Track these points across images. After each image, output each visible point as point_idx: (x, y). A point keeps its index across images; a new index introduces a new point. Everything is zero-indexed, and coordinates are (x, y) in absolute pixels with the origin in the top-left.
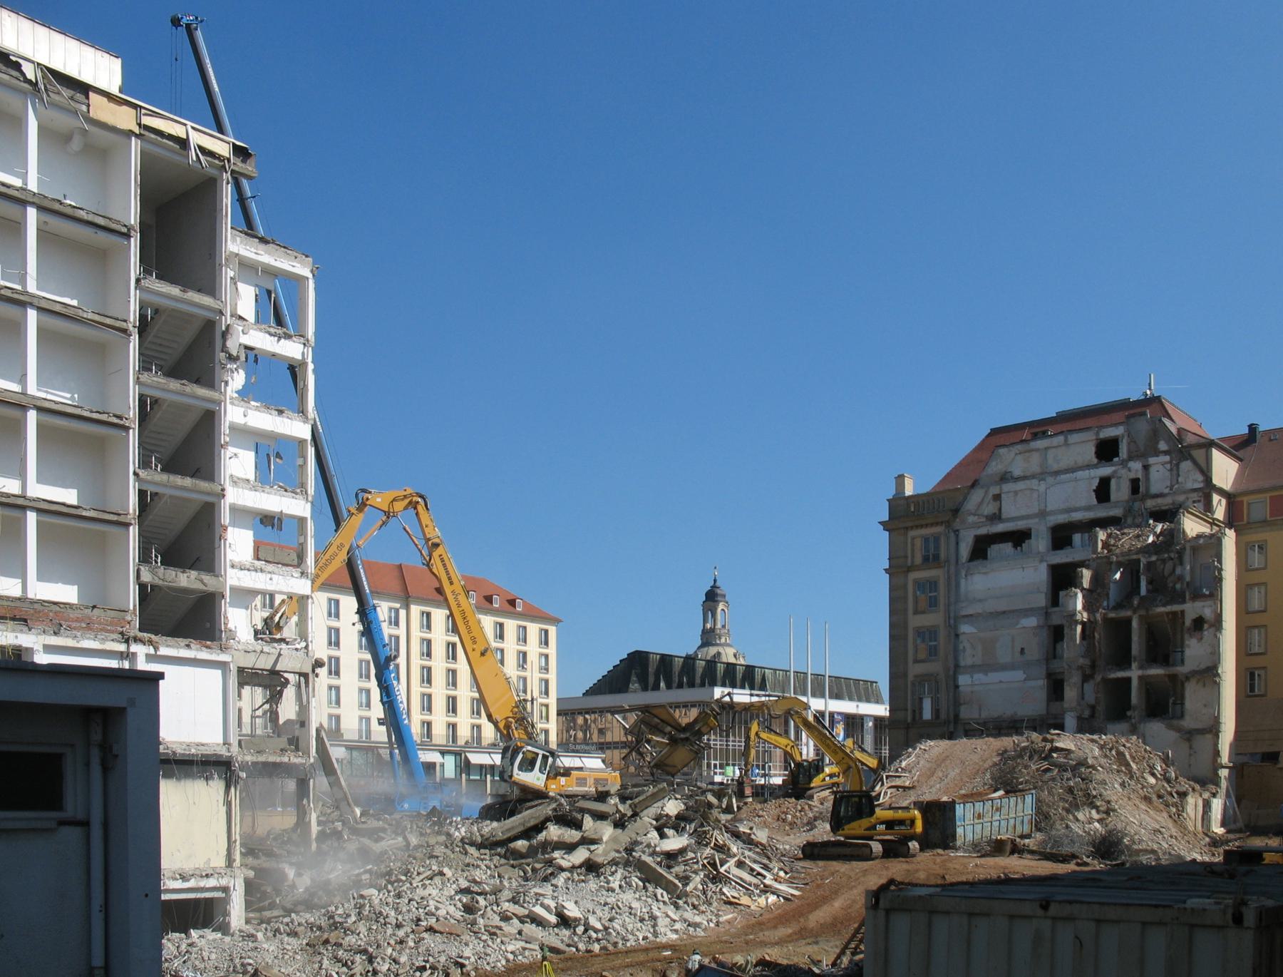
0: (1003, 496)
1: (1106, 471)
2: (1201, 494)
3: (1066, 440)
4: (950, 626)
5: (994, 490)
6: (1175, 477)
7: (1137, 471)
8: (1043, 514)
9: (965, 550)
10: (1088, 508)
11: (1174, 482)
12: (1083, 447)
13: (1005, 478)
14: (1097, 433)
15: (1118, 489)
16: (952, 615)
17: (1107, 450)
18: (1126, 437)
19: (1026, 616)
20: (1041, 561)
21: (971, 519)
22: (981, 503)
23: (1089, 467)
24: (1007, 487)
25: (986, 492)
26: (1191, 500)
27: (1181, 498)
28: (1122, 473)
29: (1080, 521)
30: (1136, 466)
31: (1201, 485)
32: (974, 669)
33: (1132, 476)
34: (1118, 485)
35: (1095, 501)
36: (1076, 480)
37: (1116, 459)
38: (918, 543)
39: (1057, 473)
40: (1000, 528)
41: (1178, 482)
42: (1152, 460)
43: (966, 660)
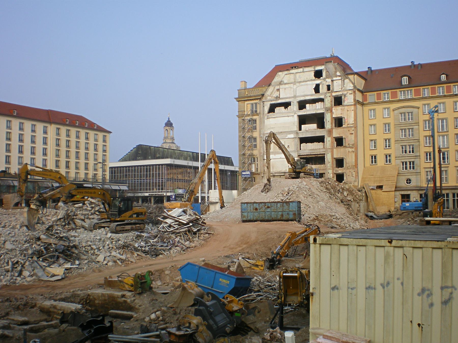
0: (280, 89)
1: (318, 81)
2: (352, 91)
3: (303, 70)
4: (261, 137)
6: (343, 85)
7: (329, 82)
8: (295, 97)
9: (267, 109)
10: (312, 95)
11: (343, 87)
12: (309, 72)
13: (281, 83)
14: (314, 68)
15: (322, 88)
16: (262, 133)
17: (318, 74)
18: (325, 70)
19: (290, 134)
20: (295, 114)
21: (269, 98)
23: (312, 80)
24: (281, 86)
25: (274, 88)
26: (349, 93)
27: (345, 92)
28: (324, 82)
29: (309, 100)
30: (329, 81)
31: (352, 88)
33: (328, 84)
34: (322, 87)
35: (314, 93)
36: (307, 85)
37: (321, 78)
38: (249, 106)
39: (300, 82)
40: (280, 101)
41: (344, 87)
42: (334, 79)
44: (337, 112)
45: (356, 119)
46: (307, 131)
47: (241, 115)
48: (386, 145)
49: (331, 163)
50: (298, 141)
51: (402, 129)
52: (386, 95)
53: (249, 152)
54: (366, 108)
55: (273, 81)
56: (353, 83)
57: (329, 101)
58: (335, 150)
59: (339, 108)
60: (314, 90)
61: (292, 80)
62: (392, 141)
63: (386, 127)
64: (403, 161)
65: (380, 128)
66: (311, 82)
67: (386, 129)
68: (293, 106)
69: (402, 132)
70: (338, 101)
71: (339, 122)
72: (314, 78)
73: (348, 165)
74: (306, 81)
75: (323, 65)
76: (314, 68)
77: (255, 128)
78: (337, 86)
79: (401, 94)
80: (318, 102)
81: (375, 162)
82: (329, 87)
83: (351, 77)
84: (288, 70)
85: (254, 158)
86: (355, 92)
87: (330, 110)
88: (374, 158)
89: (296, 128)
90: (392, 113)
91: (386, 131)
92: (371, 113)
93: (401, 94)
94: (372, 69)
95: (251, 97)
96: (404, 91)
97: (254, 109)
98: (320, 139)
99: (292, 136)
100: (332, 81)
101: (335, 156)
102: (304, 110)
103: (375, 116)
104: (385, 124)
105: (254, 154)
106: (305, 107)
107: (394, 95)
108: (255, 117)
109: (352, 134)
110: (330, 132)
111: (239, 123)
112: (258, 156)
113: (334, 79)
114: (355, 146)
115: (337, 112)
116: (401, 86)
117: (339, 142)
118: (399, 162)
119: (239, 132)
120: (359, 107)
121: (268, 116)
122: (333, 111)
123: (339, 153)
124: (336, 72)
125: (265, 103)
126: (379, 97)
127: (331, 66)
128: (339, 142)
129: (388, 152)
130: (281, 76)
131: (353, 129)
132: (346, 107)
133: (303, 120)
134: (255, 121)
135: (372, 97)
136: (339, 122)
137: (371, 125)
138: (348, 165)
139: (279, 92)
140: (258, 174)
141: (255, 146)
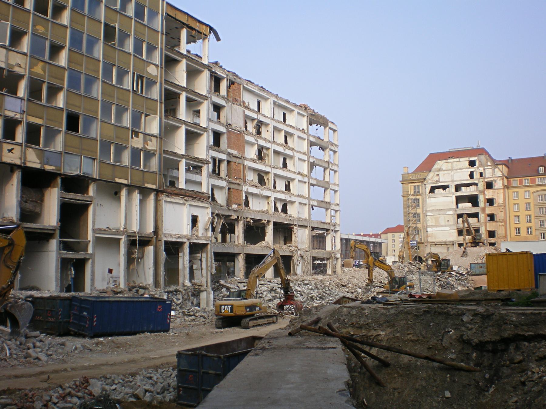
0: (440, 175)
1: (472, 169)
5: (437, 173)
8: (453, 181)
9: (428, 190)
10: (467, 180)
12: (465, 162)
13: (440, 170)
14: (469, 159)
17: (472, 164)
19: (449, 211)
20: (453, 195)
21: (430, 181)
22: (432, 177)
23: (467, 168)
24: (440, 172)
27: (495, 179)
28: (477, 170)
29: (465, 184)
32: (432, 226)
33: (480, 172)
36: (463, 172)
38: (413, 188)
39: (457, 169)
42: (486, 168)
43: (429, 224)
44: (489, 194)
45: (504, 200)
46: (464, 209)
47: (406, 195)
48: (528, 220)
49: (485, 234)
50: (456, 216)
51: (540, 208)
52: (526, 181)
53: (414, 226)
54: (511, 191)
55: (433, 168)
56: (501, 172)
57: (482, 185)
58: (488, 224)
59: (490, 191)
60: (469, 176)
61: (450, 168)
62: (533, 217)
63: (527, 206)
64: (541, 232)
65: (522, 207)
66: (466, 170)
67: (527, 208)
68: (452, 188)
69: (540, 210)
70: (489, 185)
71: (491, 202)
72: (469, 166)
73: (499, 236)
74: (462, 169)
75: (476, 156)
76: (469, 159)
77: (418, 206)
78: (488, 173)
79: (539, 180)
80: (472, 185)
81: (519, 233)
82: (481, 174)
83: (500, 167)
84: (445, 159)
85: (418, 231)
86: (503, 179)
87: (483, 192)
88: (518, 230)
89: (454, 206)
90: (532, 195)
91: (527, 209)
92: (515, 194)
93: (539, 180)
94: (513, 158)
95: (414, 180)
96: (541, 178)
97: (417, 190)
98: (476, 215)
99: (451, 212)
100: (484, 169)
101: (488, 229)
102: (460, 192)
103: (518, 197)
104: (526, 204)
105: (418, 227)
106: (461, 190)
107: (533, 181)
108: (418, 197)
109: (502, 211)
110: (484, 210)
111: (404, 201)
112: (421, 228)
113: (486, 168)
114: (504, 221)
115: (489, 194)
116: (538, 174)
117: (492, 217)
118: (538, 233)
119: (404, 208)
120: (506, 190)
121: (429, 196)
122: (486, 193)
123: (491, 226)
124: (487, 162)
125: (426, 185)
126: (521, 182)
127: (483, 157)
128: (492, 217)
129: (529, 225)
130: (440, 164)
131: (503, 207)
132: (496, 190)
133: (459, 199)
134: (418, 200)
135: (515, 182)
136: (491, 202)
137: (515, 204)
138: (499, 236)
139: (438, 177)
140: (422, 243)
141: (419, 220)
